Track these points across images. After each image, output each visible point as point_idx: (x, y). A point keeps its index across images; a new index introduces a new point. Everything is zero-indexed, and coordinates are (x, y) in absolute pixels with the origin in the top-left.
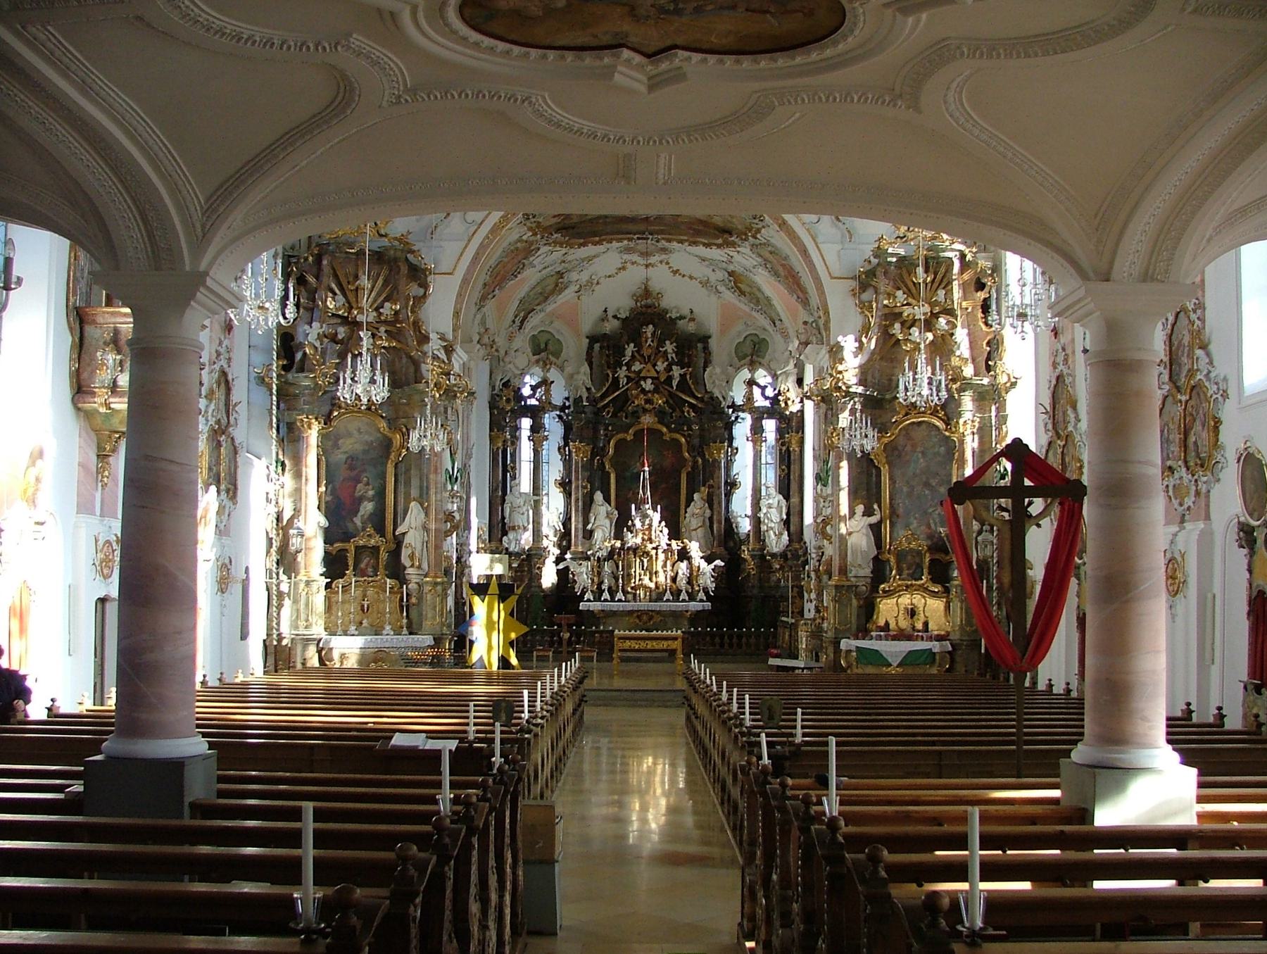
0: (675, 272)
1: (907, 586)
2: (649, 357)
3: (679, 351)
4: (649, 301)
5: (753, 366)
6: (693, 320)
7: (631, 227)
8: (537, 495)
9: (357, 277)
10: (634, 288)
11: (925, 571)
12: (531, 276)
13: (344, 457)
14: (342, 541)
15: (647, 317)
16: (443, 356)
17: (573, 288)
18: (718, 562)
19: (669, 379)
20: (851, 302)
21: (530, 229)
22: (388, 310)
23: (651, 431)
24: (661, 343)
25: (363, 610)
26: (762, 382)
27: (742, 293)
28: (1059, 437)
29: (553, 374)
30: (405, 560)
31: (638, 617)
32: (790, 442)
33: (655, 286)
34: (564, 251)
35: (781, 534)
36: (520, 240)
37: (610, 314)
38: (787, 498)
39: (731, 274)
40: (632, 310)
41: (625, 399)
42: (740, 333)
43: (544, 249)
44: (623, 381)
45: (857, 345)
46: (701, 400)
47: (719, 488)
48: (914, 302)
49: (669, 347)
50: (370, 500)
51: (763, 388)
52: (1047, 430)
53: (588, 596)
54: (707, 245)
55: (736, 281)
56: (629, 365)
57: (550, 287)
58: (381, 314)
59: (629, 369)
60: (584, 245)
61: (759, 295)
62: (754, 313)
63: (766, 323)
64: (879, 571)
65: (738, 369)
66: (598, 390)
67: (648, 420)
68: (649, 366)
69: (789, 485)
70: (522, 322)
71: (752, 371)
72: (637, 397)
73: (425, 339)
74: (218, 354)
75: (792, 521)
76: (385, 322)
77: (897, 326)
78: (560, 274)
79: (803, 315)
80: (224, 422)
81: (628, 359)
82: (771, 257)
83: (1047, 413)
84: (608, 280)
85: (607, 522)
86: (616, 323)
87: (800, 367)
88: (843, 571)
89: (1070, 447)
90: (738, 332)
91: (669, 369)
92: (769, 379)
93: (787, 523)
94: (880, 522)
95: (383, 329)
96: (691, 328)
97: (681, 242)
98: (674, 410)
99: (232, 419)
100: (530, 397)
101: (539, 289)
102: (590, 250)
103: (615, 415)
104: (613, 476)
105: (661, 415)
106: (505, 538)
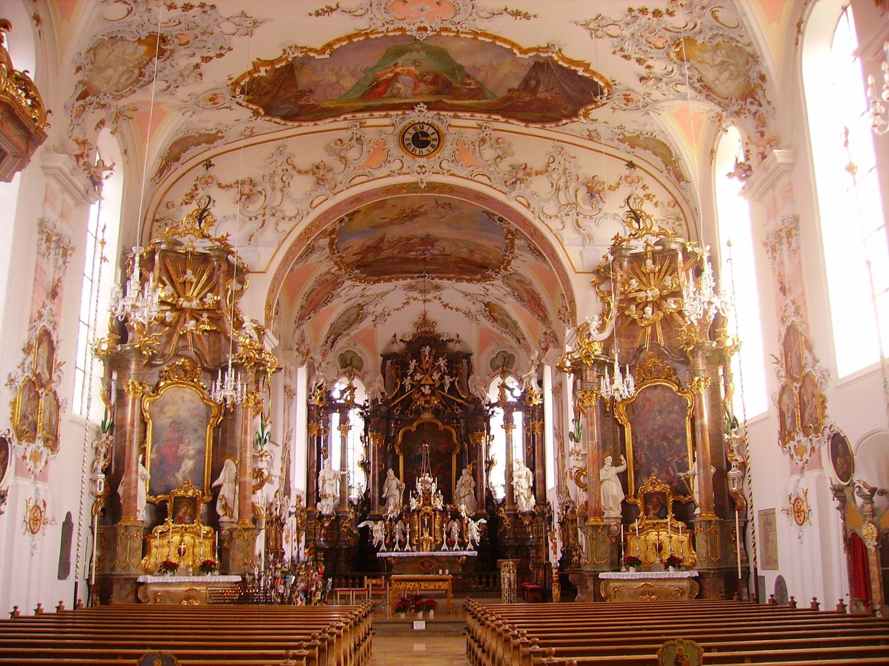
0: (445, 306)
1: (654, 525)
2: (427, 370)
3: (449, 365)
4: (427, 329)
5: (504, 374)
6: (459, 342)
8: (344, 470)
9: (185, 273)
10: (416, 320)
11: (670, 510)
12: (337, 307)
13: (168, 421)
14: (165, 493)
15: (425, 342)
16: (255, 337)
17: (370, 318)
18: (483, 521)
19: (442, 386)
20: (592, 293)
21: (336, 263)
22: (210, 299)
23: (429, 424)
24: (436, 359)
25: (179, 552)
26: (510, 386)
27: (495, 320)
28: (794, 380)
30: (220, 511)
31: (422, 563)
32: (534, 428)
33: (431, 317)
34: (363, 286)
35: (529, 498)
36: (328, 272)
37: (398, 338)
38: (533, 470)
39: (487, 305)
40: (414, 335)
41: (409, 401)
44: (408, 387)
45: (601, 322)
47: (481, 465)
48: (644, 288)
49: (442, 362)
50: (190, 459)
51: (511, 390)
52: (779, 377)
53: (383, 547)
54: (469, 281)
55: (491, 310)
56: (412, 376)
57: (354, 317)
58: (204, 303)
59: (412, 378)
60: (378, 281)
61: (507, 320)
62: (504, 335)
63: (513, 342)
64: (628, 511)
65: (493, 377)
66: (389, 395)
67: (427, 416)
68: (427, 376)
69: (534, 458)
70: (333, 343)
71: (503, 378)
72: (418, 399)
73: (239, 324)
74: (41, 316)
75: (538, 488)
76: (208, 310)
77: (633, 307)
78: (361, 307)
79: (541, 328)
80: (46, 376)
81: (411, 371)
82: (518, 286)
83: (778, 362)
84: (396, 309)
85: (397, 493)
86: (403, 345)
87: (540, 369)
88: (599, 513)
89: (809, 388)
91: (442, 378)
92: (516, 383)
93: (533, 489)
94: (626, 471)
95: (205, 315)
96: (457, 347)
97: (449, 279)
98: (446, 409)
99: (55, 377)
100: (340, 399)
101: (345, 318)
102: (382, 287)
103: (402, 412)
104: (401, 459)
105: (436, 412)
106: (319, 504)
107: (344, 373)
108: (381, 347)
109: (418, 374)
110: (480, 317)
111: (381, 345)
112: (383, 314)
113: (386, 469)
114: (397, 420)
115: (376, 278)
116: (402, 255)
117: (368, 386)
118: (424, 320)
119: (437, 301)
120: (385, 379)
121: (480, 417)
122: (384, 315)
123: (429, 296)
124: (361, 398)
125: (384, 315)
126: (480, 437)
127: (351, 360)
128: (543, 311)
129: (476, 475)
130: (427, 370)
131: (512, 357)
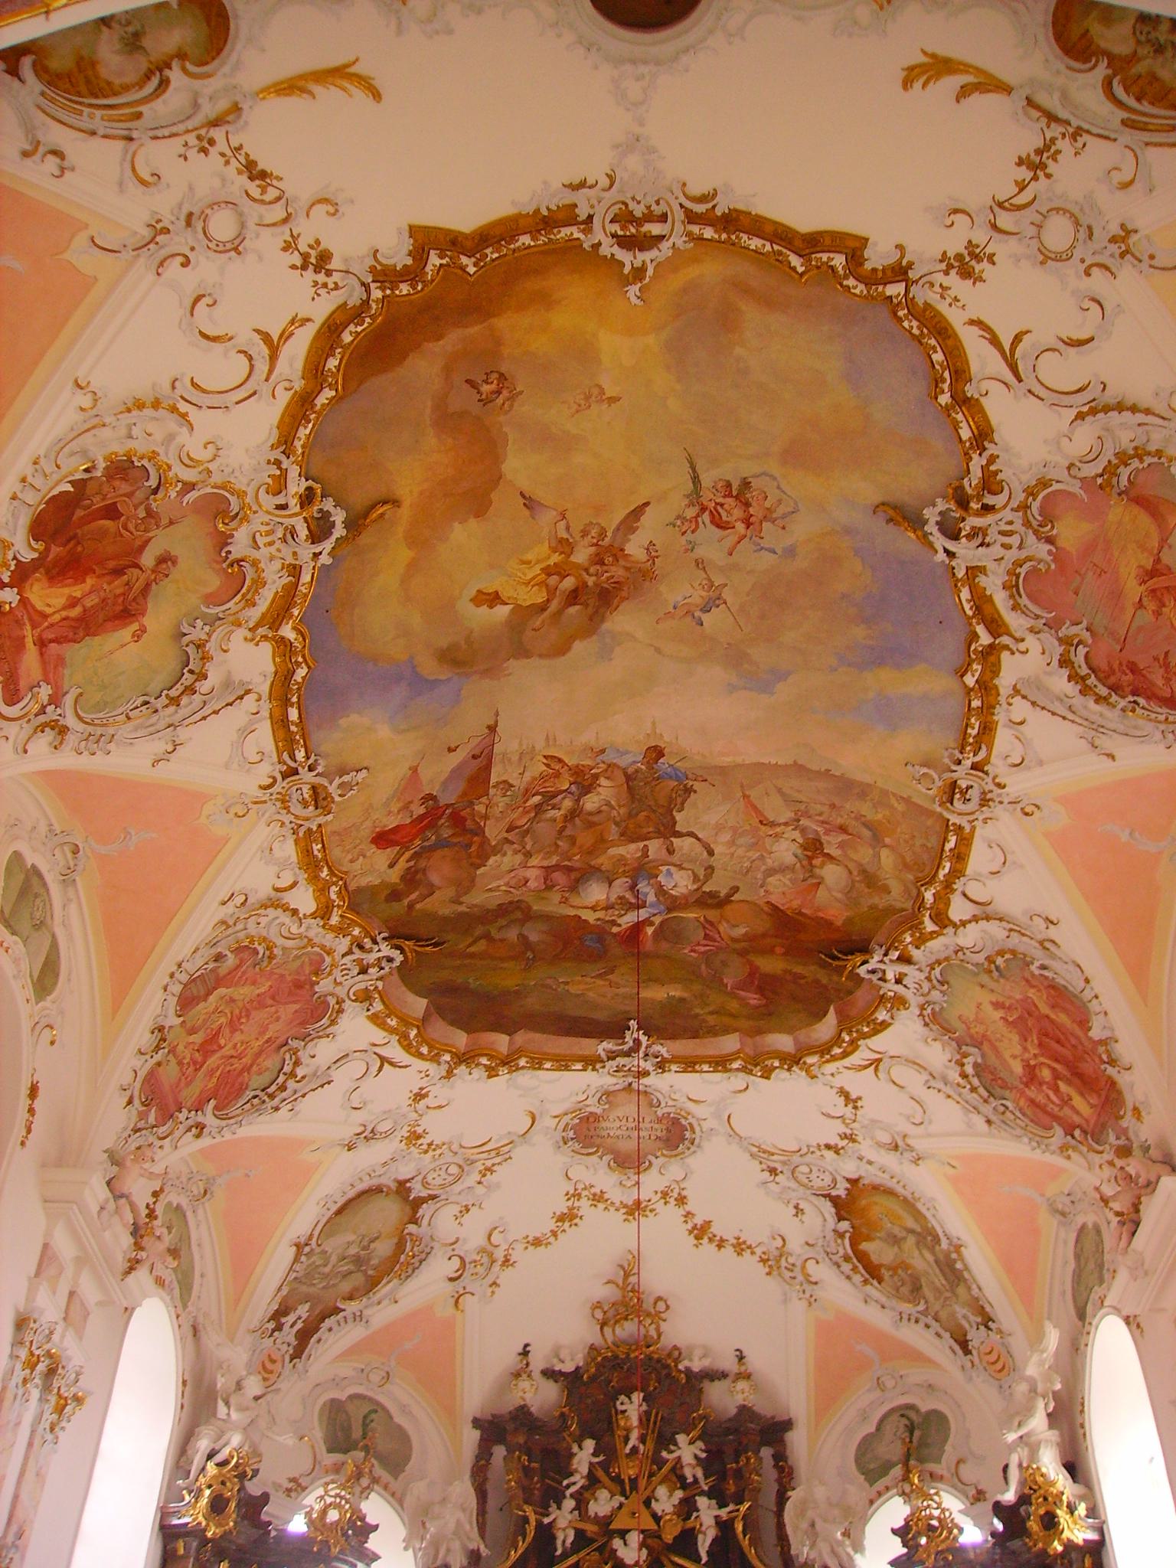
6: (748, 1376)
7: (589, 989)
19: (686, 1542)
27: (873, 1272)
29: (375, 1508)
34: (415, 1072)
37: (538, 1362)
39: (850, 1204)
43: (355, 1029)
44: (565, 1537)
56: (581, 1503)
59: (581, 1503)
60: (464, 1058)
61: (921, 1261)
78: (410, 1201)
107: (337, 1468)
110: (822, 1271)
111: (479, 1385)
112: (487, 1250)
115: (461, 1039)
116: (553, 905)
117: (418, 1521)
118: (629, 1300)
119: (670, 1214)
120: (482, 1511)
122: (491, 1260)
123: (652, 1182)
125: (491, 1260)
127: (366, 1422)
128: (1087, 1083)
130: (634, 1482)
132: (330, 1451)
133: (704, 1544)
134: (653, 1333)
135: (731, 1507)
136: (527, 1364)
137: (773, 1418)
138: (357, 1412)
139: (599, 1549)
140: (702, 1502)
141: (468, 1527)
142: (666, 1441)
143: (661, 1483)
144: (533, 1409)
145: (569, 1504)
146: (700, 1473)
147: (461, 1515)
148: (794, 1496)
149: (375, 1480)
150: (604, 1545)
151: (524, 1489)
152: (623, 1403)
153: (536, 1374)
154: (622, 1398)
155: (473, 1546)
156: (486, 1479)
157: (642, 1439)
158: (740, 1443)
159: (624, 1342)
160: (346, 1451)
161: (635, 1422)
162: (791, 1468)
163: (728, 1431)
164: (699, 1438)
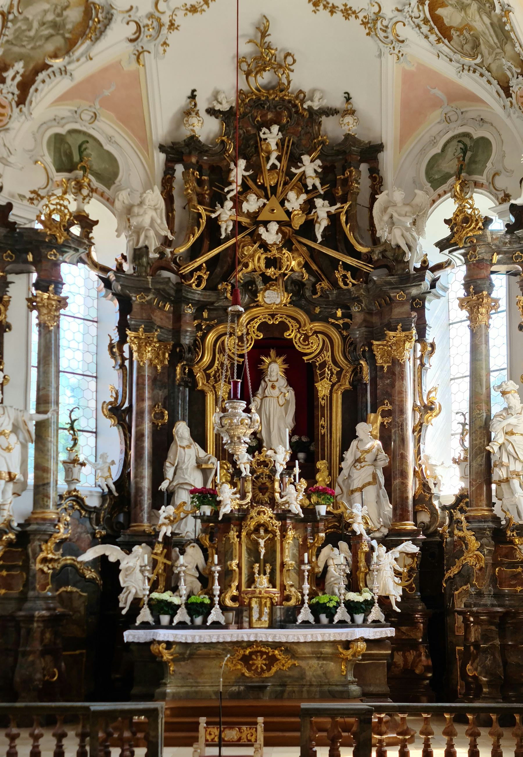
2: (274, 189)
6: (352, 112)
19: (308, 228)
42: (433, 142)
44: (226, 227)
46: (368, 259)
49: (310, 167)
81: (235, 188)
90: (436, 131)
96: (349, 125)
98: (319, 280)
103: (211, 287)
105: (296, 288)
108: (161, 126)
109: (252, 197)
113: (172, 423)
114: (200, 307)
121: (398, 295)
124: (110, 245)
126: (400, 344)
129: (391, 437)
130: (274, 189)
131: (484, 144)
132: (58, 170)
133: (319, 231)
134: (285, 81)
135: (339, 205)
136: (195, 105)
137: (370, 142)
138: (74, 142)
139: (251, 234)
140: (319, 202)
141: (159, 221)
142: (295, 160)
143: (291, 190)
144: (201, 139)
145: (229, 204)
146: (317, 183)
147: (154, 214)
148: (381, 198)
149: (92, 190)
150: (254, 231)
151: (198, 195)
152: (264, 133)
153: (202, 113)
154: (264, 129)
155: (163, 233)
156: (172, 187)
157: (279, 158)
158: (346, 161)
159: (265, 87)
160: (70, 171)
161: (273, 147)
162: (381, 179)
163: (339, 153)
164: (319, 157)
